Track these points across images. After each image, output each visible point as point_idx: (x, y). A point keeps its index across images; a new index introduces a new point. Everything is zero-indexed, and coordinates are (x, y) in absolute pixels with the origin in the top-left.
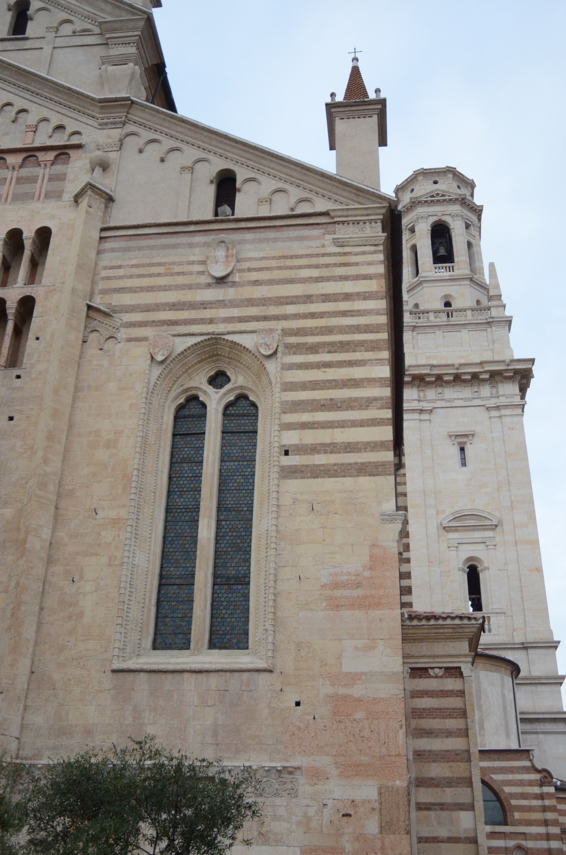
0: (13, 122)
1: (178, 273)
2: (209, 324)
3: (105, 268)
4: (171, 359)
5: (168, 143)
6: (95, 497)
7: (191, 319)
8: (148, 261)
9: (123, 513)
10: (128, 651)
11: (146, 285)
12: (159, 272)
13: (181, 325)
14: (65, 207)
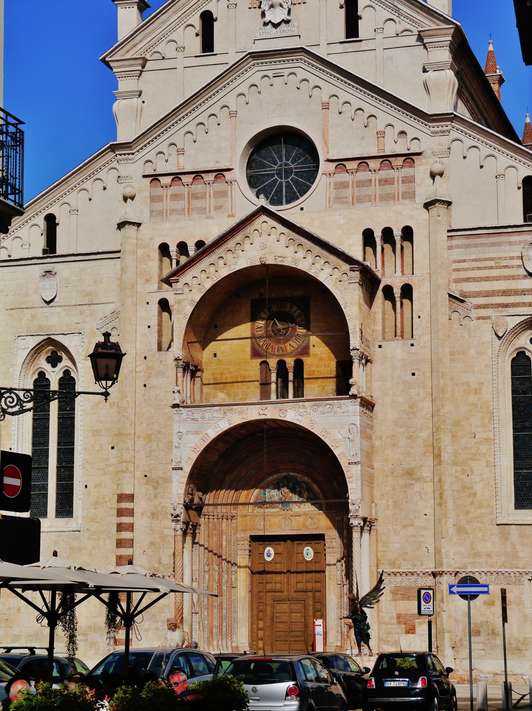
0: (365, 127)
1: (504, 266)
2: (528, 306)
3: (455, 262)
4: (507, 333)
5: (485, 150)
6: (473, 425)
7: (516, 303)
8: (482, 256)
9: (491, 435)
10: (503, 513)
11: (484, 276)
12: (491, 265)
13: (510, 307)
14: (418, 209)
